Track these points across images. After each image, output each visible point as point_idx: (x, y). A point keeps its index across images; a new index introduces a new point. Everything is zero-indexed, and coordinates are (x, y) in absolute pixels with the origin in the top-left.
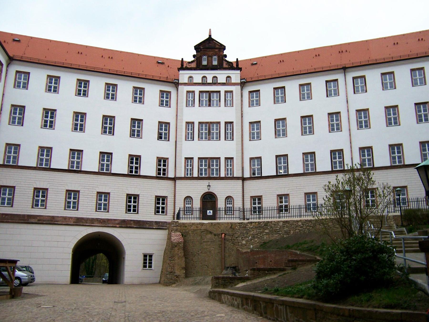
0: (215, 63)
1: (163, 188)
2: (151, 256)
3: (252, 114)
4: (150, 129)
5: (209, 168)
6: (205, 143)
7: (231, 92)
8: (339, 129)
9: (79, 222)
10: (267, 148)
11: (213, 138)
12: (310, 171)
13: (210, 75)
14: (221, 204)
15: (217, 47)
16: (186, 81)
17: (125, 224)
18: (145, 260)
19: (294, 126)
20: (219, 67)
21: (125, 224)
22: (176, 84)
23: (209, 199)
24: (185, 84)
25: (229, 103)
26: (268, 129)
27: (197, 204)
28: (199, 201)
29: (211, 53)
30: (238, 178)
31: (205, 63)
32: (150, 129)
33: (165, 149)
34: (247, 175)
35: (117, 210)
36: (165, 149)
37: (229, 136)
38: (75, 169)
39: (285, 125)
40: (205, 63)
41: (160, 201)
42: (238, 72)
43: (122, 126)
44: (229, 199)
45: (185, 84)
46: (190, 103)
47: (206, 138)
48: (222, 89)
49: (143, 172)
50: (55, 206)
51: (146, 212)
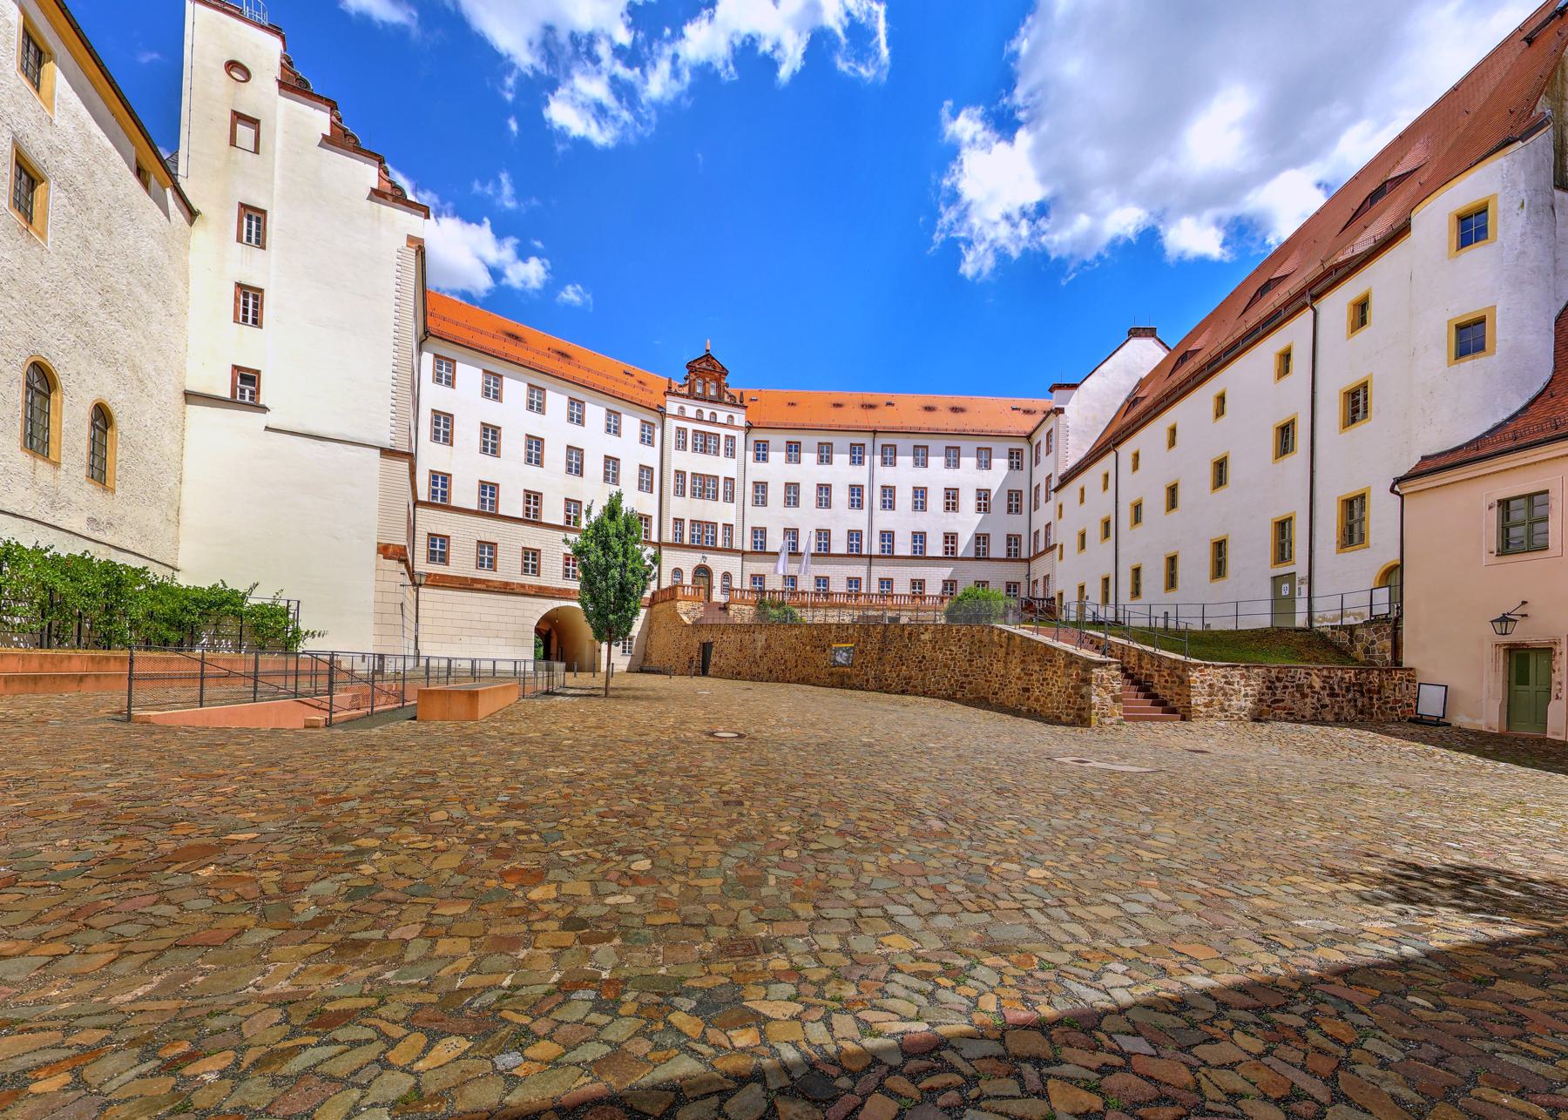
3: (758, 471)
6: (698, 502)
8: (860, 506)
10: (774, 518)
14: (717, 581)
16: (675, 412)
19: (808, 494)
20: (717, 400)
22: (661, 412)
23: (703, 572)
24: (675, 417)
25: (731, 453)
27: (687, 580)
37: (730, 497)
39: (797, 493)
40: (699, 390)
44: (727, 576)
45: (675, 417)
46: (681, 446)
48: (723, 432)
50: (509, 568)
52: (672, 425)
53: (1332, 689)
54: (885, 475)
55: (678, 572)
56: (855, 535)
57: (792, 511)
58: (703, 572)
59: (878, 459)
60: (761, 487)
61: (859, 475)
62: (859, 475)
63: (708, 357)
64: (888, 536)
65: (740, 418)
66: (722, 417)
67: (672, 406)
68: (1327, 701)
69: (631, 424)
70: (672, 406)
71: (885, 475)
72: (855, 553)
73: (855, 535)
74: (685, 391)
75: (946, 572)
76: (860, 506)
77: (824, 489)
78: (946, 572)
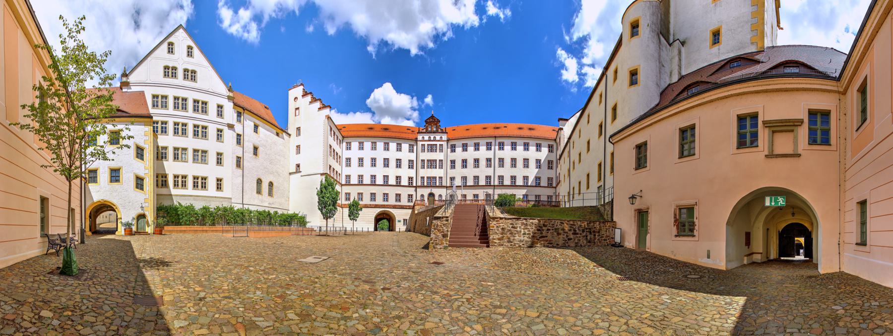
1: (411, 191)
3: (452, 156)
4: (405, 164)
5: (431, 182)
6: (430, 170)
9: (376, 206)
12: (476, 186)
14: (437, 198)
17: (394, 207)
20: (437, 132)
22: (416, 140)
23: (431, 195)
25: (441, 151)
26: (459, 164)
27: (426, 199)
33: (412, 173)
35: (392, 201)
36: (412, 173)
37: (441, 167)
38: (373, 184)
41: (410, 196)
44: (440, 196)
46: (423, 151)
48: (438, 143)
52: (420, 143)
53: (575, 230)
54: (500, 154)
55: (422, 196)
56: (488, 178)
57: (465, 170)
58: (431, 195)
59: (497, 147)
61: (490, 154)
62: (490, 154)
63: (432, 117)
64: (501, 178)
65: (445, 137)
66: (438, 138)
67: (420, 137)
68: (572, 236)
69: (405, 146)
70: (420, 137)
71: (500, 154)
72: (488, 185)
73: (488, 178)
75: (524, 191)
78: (524, 191)
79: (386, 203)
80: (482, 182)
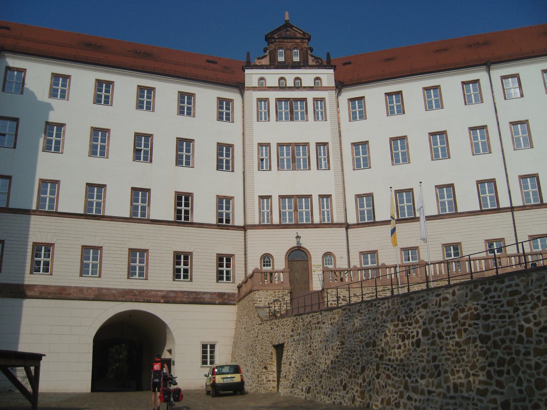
0: (296, 59)
1: (227, 242)
2: (213, 346)
5: (297, 211)
6: (288, 174)
7: (322, 100)
8: (487, 149)
9: (100, 295)
11: (299, 167)
12: (450, 212)
13: (290, 75)
15: (299, 36)
16: (255, 84)
17: (170, 298)
18: (204, 352)
20: (303, 64)
21: (170, 298)
23: (298, 256)
24: (254, 89)
26: (380, 152)
27: (280, 263)
28: (284, 260)
29: (289, 45)
30: (339, 225)
31: (281, 59)
32: (205, 154)
33: (228, 183)
34: (352, 219)
35: (160, 278)
36: (228, 183)
37: (323, 163)
38: (93, 213)
39: (405, 147)
41: (224, 261)
42: (332, 71)
43: (164, 149)
45: (254, 89)
47: (288, 167)
48: (310, 95)
49: (196, 218)
51: (204, 279)
56: (486, 185)
58: (298, 256)
60: (361, 147)
73: (486, 185)
74: (266, 61)
76: (487, 149)
77: (439, 137)
79: (137, 284)
80: (468, 200)
